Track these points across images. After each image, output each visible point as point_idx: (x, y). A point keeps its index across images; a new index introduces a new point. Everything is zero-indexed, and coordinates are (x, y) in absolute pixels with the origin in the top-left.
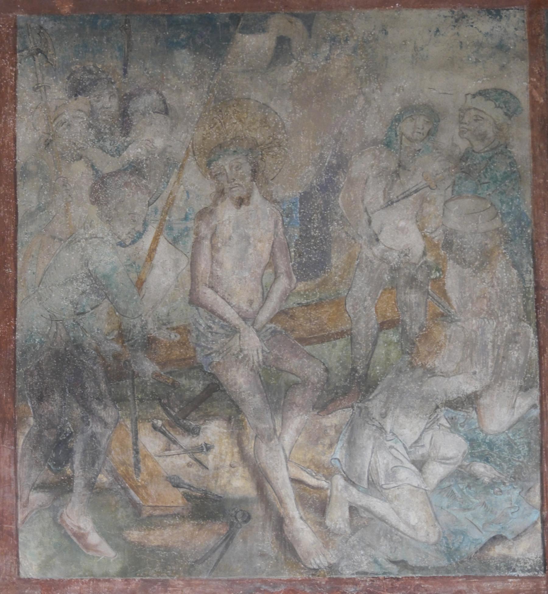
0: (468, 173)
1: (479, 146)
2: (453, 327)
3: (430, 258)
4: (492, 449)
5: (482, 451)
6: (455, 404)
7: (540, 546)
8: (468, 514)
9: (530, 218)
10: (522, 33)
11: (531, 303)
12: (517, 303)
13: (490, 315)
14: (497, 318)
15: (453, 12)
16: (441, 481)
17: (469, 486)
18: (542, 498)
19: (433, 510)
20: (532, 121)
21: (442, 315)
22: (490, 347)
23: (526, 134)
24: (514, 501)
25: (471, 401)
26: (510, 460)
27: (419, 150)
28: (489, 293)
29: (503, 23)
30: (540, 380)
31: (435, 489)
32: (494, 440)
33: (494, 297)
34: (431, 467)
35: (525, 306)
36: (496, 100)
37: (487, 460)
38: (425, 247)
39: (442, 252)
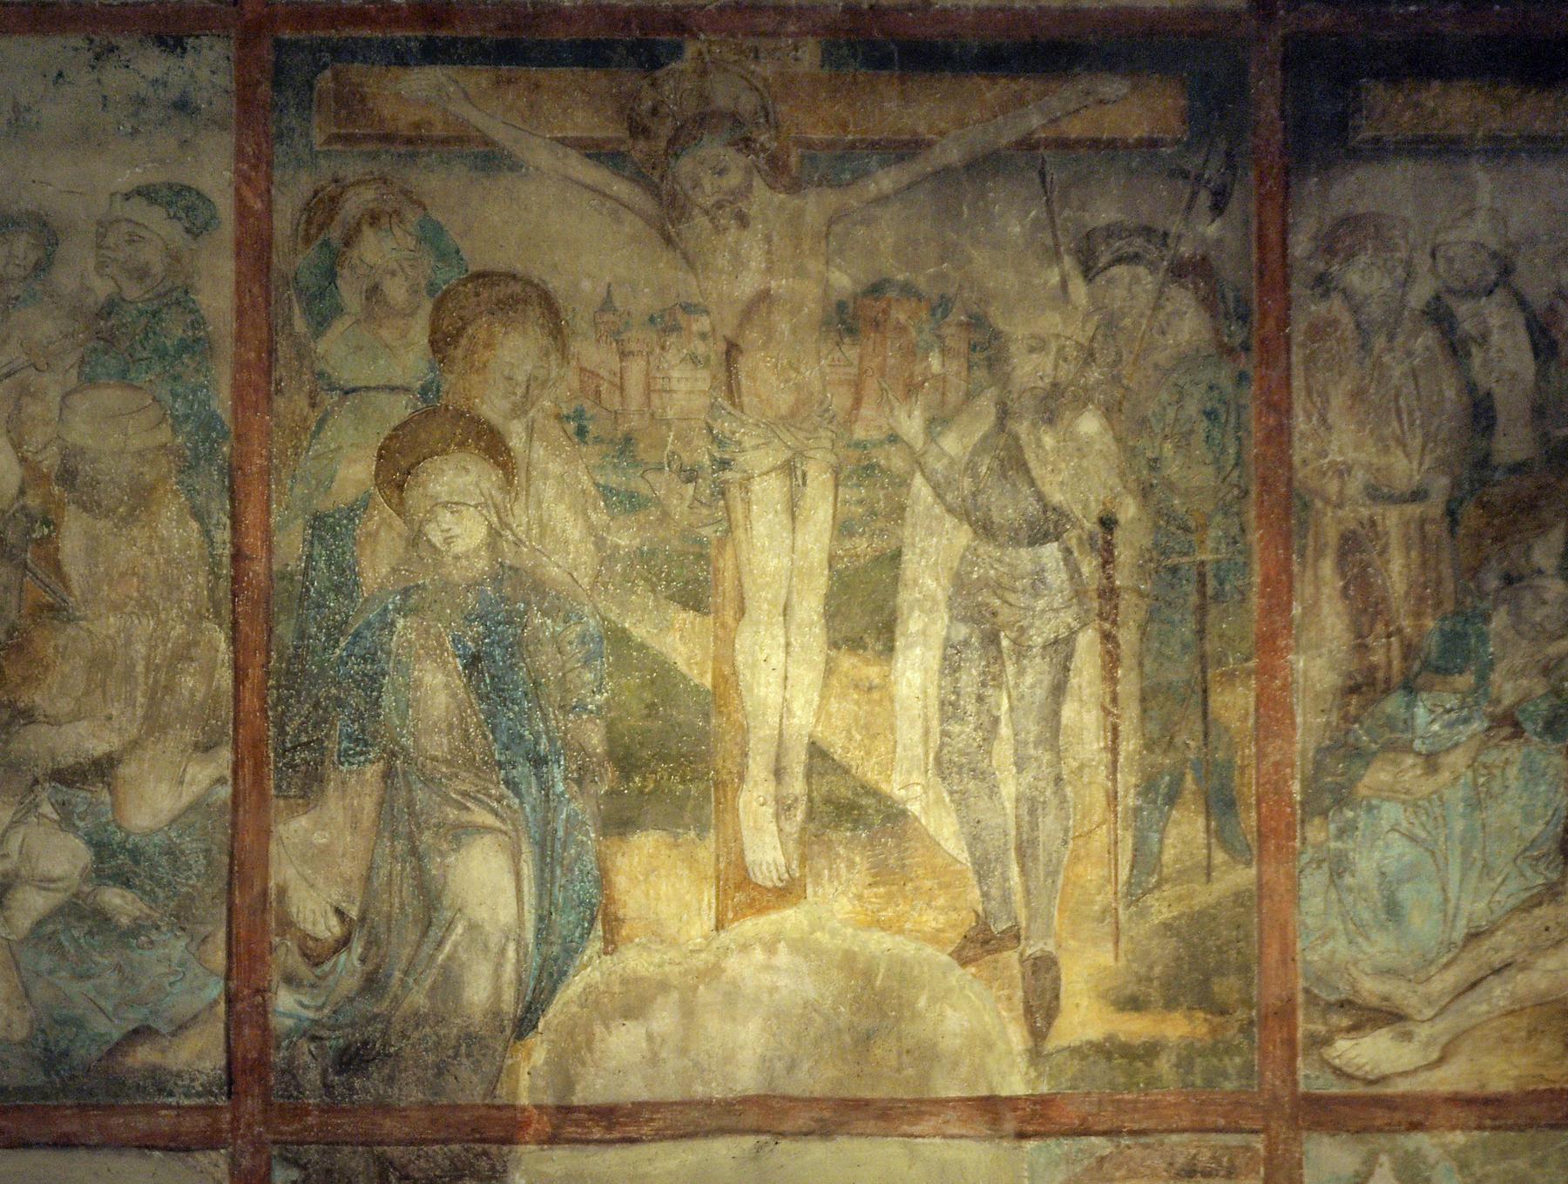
0: (110, 340)
1: (133, 291)
2: (71, 630)
3: (33, 502)
4: (137, 863)
5: (120, 867)
6: (69, 777)
7: (222, 1048)
8: (89, 984)
9: (229, 425)
10: (225, 80)
11: (224, 584)
12: (197, 585)
13: (143, 608)
14: (156, 614)
15: (92, 41)
16: (39, 923)
17: (90, 933)
18: (229, 955)
19: (20, 976)
20: (239, 244)
21: (51, 607)
22: (140, 668)
23: (226, 267)
24: (175, 961)
25: (102, 770)
26: (169, 883)
27: (17, 298)
28: (144, 566)
29: (189, 60)
30: (236, 730)
31: (26, 938)
32: (142, 844)
33: (153, 574)
34: (19, 896)
35: (211, 590)
36: (170, 204)
37: (127, 884)
38: (23, 481)
39: (56, 490)
